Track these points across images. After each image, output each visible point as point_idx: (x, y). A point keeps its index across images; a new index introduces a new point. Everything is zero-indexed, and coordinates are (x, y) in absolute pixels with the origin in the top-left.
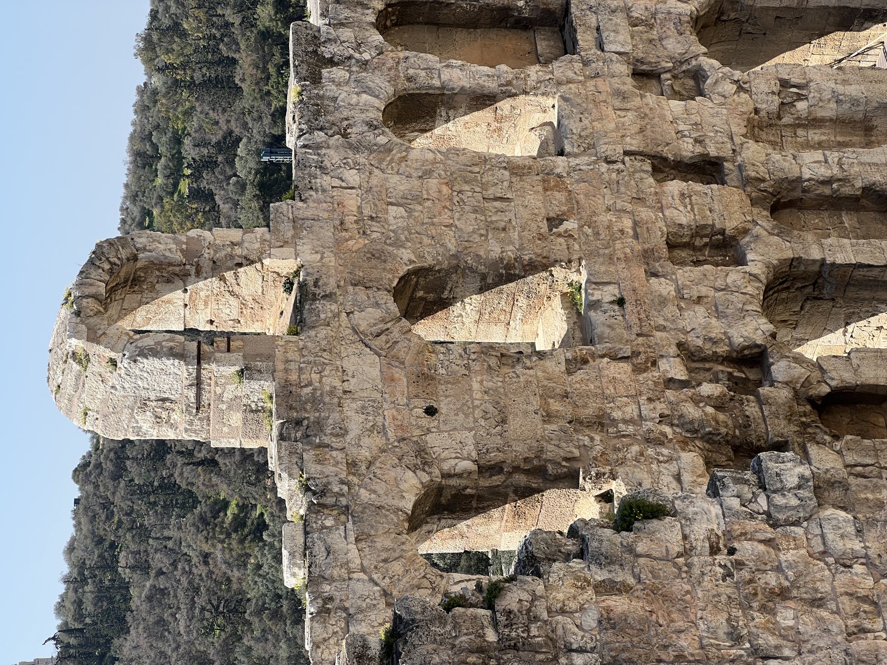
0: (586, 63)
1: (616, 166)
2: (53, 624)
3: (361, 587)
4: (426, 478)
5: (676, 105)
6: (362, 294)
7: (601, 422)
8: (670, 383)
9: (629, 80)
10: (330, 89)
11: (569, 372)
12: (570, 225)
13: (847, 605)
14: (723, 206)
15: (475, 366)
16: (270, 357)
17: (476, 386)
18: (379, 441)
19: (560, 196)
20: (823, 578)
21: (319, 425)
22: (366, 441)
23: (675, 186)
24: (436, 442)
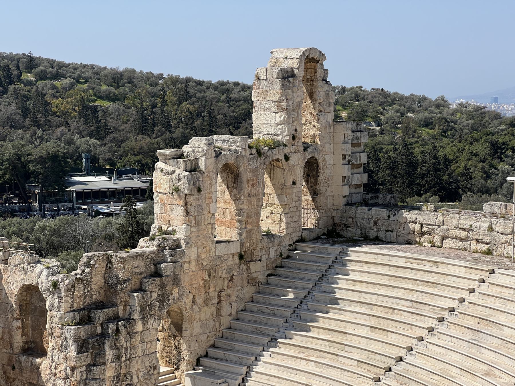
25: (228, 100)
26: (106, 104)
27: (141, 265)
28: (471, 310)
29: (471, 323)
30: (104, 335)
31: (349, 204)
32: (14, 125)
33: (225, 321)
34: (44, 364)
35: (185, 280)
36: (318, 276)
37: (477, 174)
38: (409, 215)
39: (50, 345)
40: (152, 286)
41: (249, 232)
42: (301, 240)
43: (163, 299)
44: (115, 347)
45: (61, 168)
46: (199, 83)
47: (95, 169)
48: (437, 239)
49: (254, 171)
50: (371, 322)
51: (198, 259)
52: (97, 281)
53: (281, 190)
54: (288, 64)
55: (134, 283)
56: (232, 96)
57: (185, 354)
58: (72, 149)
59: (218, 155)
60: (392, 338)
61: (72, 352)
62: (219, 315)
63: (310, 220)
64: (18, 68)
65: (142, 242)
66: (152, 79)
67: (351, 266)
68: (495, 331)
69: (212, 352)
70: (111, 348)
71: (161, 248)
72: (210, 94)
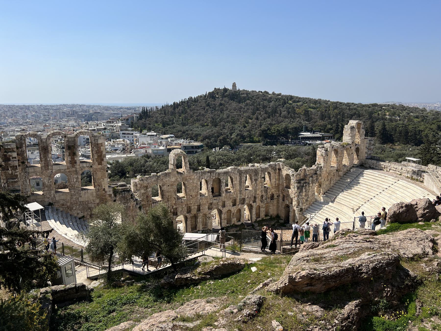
2: (241, 89)
3: (149, 181)
7: (168, 201)
8: (173, 207)
10: (207, 174)
14: (194, 212)
18: (165, 181)
23: (196, 207)
25: (349, 109)
26: (312, 110)
27: (312, 171)
28: (391, 189)
29: (390, 192)
30: (303, 186)
31: (367, 159)
32: (285, 117)
33: (332, 185)
34: (290, 190)
35: (323, 175)
36: (355, 176)
37: (431, 136)
38: (382, 163)
39: (291, 187)
40: (315, 176)
41: (339, 165)
42: (353, 167)
43: (317, 179)
44: (305, 189)
45: (297, 130)
46: (341, 103)
47: (307, 130)
48: (388, 170)
49: (342, 151)
50: (367, 189)
51: (326, 171)
52: (302, 174)
53: (349, 155)
54: (353, 125)
55: (311, 175)
56: (351, 108)
57: (321, 191)
58: (301, 125)
59: (333, 147)
60: (371, 194)
61: (296, 189)
62: (330, 183)
63: (356, 162)
64: (287, 99)
65: (313, 166)
66: (326, 102)
67: (364, 175)
68: (395, 195)
69: (328, 191)
71: (317, 168)
72: (344, 107)
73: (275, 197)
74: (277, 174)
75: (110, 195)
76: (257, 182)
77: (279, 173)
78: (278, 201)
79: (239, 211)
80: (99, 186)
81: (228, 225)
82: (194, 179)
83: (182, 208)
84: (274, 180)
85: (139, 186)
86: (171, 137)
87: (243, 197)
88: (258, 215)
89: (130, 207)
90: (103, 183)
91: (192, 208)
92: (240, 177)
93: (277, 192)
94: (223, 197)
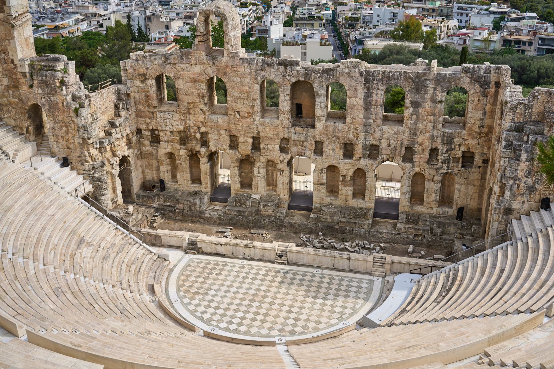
0: (288, 128)
1: (255, 129)
4: (173, 78)
5: (277, 147)
6: (215, 68)
7: (189, 113)
8: (199, 128)
9: (282, 137)
11: (201, 110)
12: (238, 116)
13: (67, 138)
15: (199, 91)
16: (197, 50)
17: (194, 90)
18: (180, 70)
19: (246, 115)
20: (70, 135)
21: (182, 59)
22: (179, 68)
23: (250, 140)
24: (180, 81)
52: (537, 107)
70: (526, 151)
73: (478, 161)
74: (490, 99)
75: (24, 74)
76: (421, 110)
77: (496, 95)
78: (484, 174)
79: (360, 174)
80: (4, 53)
81: (328, 200)
82: (243, 76)
83: (219, 134)
84: (479, 114)
85: (130, 71)
86: (531, 18)
87: (374, 142)
88: (416, 196)
89: (57, 103)
90: (9, 48)
91: (241, 140)
92: (368, 89)
93: (485, 150)
94: (317, 130)
